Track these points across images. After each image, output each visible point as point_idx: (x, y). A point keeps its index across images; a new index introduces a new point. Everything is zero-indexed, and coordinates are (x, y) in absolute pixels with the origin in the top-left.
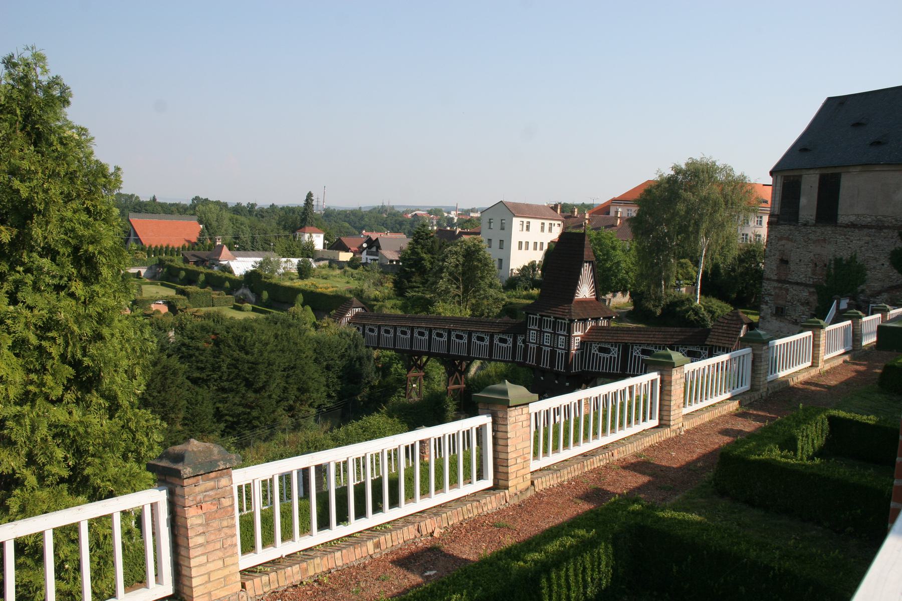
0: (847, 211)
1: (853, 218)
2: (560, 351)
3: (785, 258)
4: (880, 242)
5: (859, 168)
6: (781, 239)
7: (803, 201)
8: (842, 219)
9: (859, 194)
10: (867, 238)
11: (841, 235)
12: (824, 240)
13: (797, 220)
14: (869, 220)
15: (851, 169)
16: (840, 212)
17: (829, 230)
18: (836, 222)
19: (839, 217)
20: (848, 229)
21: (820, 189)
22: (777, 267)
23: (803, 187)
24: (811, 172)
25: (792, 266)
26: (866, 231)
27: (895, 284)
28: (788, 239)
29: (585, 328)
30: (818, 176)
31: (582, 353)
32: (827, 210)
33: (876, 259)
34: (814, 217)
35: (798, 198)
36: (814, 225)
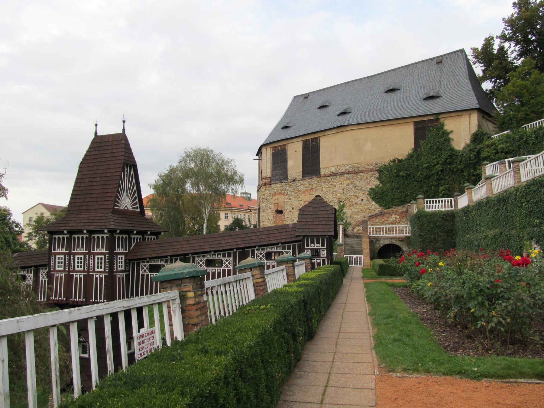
0: (327, 163)
1: (333, 169)
2: (98, 275)
3: (279, 209)
4: (357, 183)
5: (334, 131)
6: (275, 194)
7: (290, 163)
8: (323, 172)
9: (334, 153)
10: (348, 182)
11: (325, 183)
12: (312, 189)
13: (286, 178)
14: (347, 168)
15: (328, 133)
16: (322, 166)
17: (314, 181)
18: (320, 175)
19: (321, 170)
20: (331, 177)
21: (303, 151)
22: (274, 217)
23: (289, 153)
24: (295, 140)
25: (286, 214)
26: (346, 176)
27: (373, 214)
28: (280, 194)
29: (130, 245)
30: (301, 143)
31: (127, 276)
32: (311, 165)
33: (356, 196)
34: (301, 174)
35: (285, 161)
36: (302, 180)
